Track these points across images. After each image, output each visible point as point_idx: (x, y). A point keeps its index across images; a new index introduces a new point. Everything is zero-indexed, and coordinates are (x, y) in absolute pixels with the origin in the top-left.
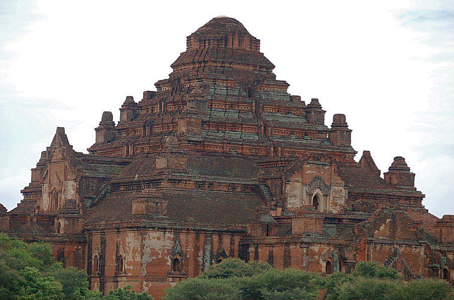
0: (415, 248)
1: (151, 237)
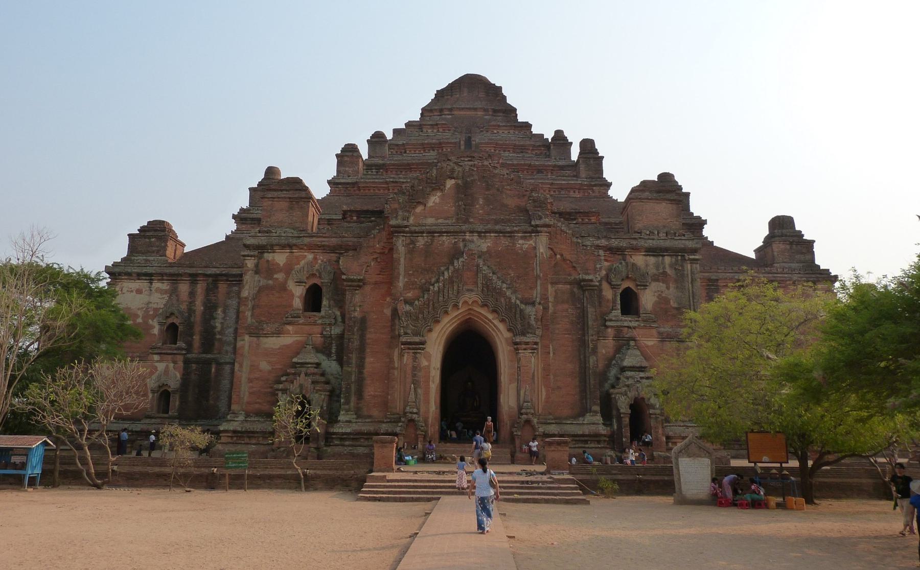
0: (522, 238)
1: (125, 290)
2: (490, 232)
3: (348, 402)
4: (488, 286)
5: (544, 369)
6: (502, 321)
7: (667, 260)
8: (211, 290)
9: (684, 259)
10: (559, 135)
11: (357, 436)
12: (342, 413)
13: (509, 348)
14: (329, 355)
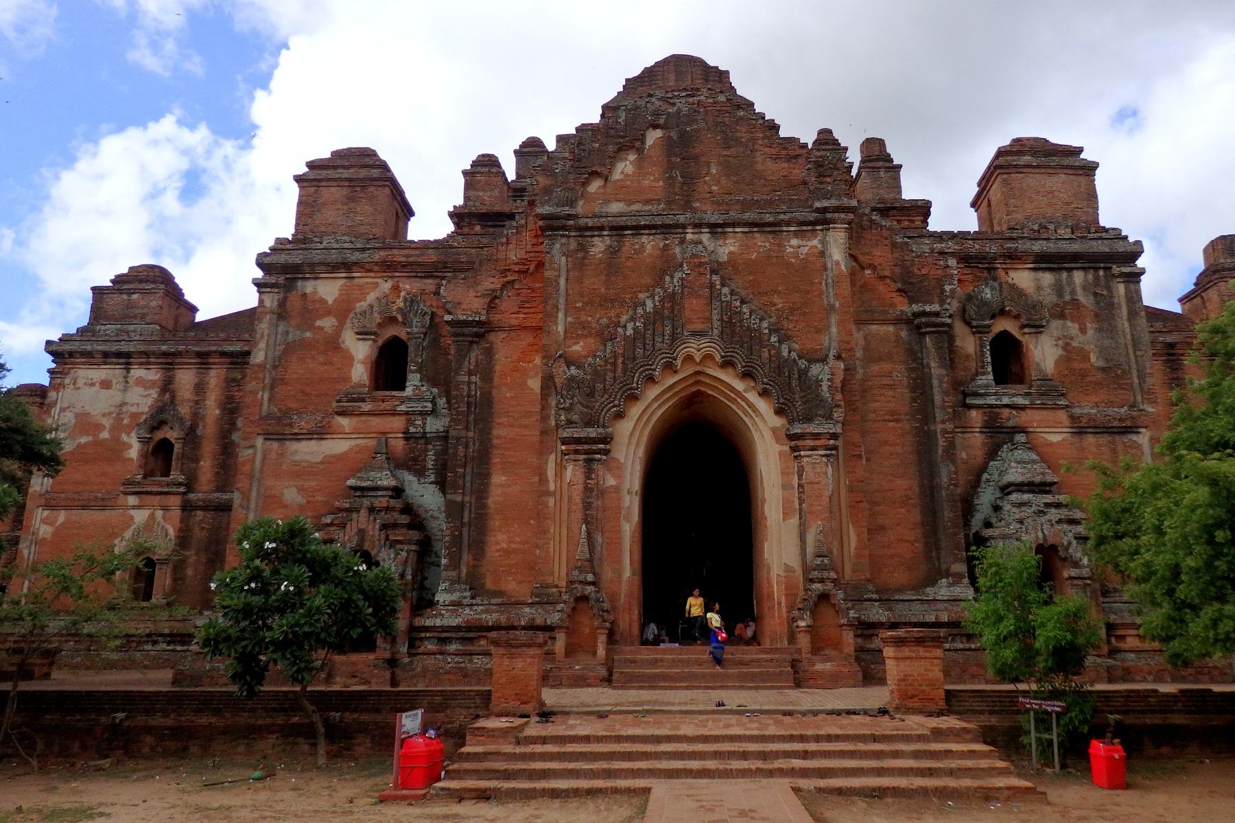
0: (796, 234)
1: (80, 383)
2: (733, 225)
3: (455, 564)
4: (730, 324)
5: (851, 490)
6: (764, 394)
7: (1078, 277)
11: (471, 633)
12: (442, 586)
13: (778, 448)
14: (420, 473)
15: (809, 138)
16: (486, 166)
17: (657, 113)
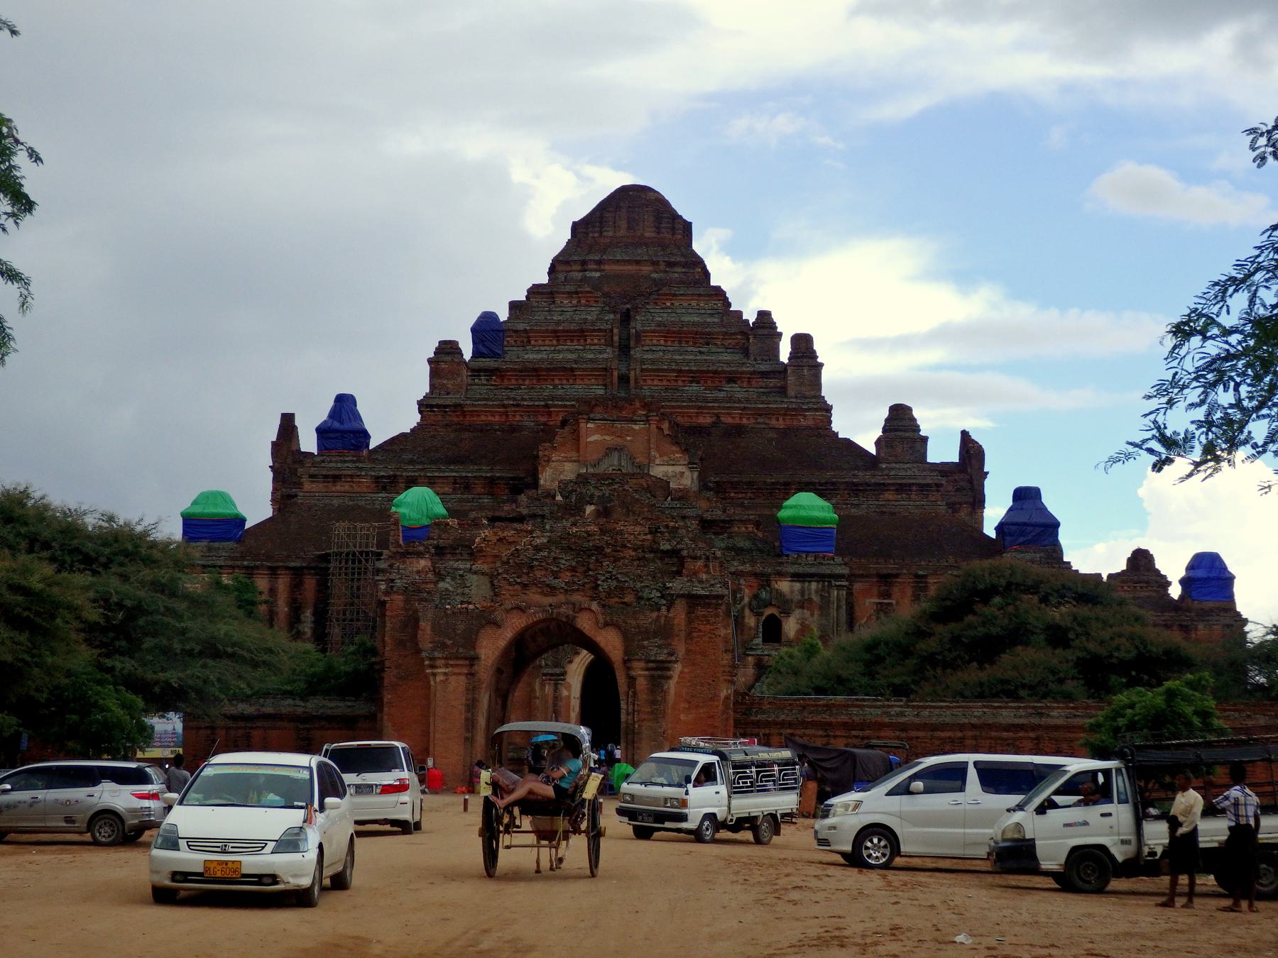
7: (814, 586)
8: (296, 586)
9: (830, 585)
10: (764, 316)
15: (750, 316)
16: (448, 354)
17: (592, 496)
